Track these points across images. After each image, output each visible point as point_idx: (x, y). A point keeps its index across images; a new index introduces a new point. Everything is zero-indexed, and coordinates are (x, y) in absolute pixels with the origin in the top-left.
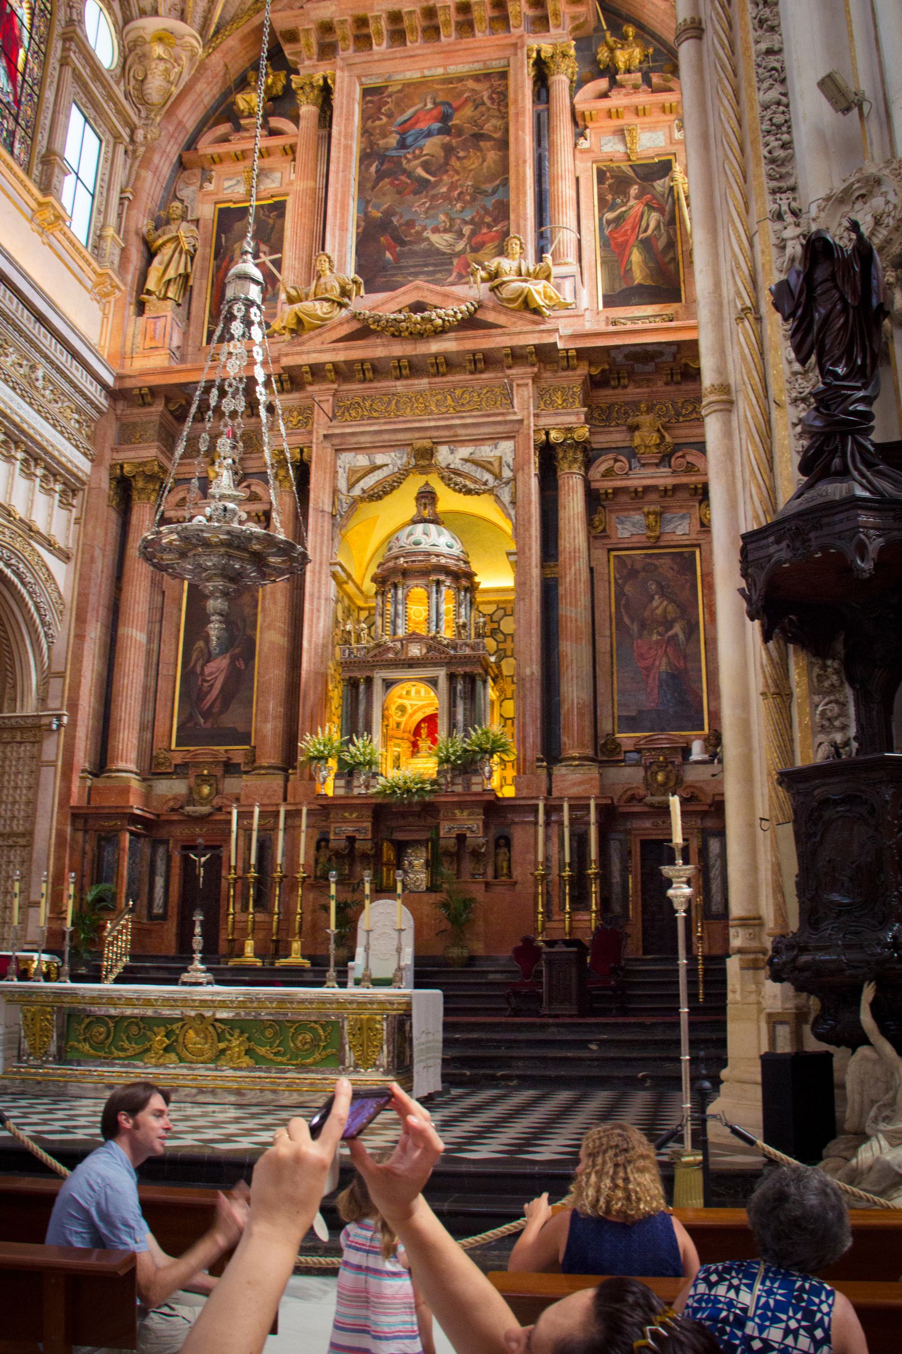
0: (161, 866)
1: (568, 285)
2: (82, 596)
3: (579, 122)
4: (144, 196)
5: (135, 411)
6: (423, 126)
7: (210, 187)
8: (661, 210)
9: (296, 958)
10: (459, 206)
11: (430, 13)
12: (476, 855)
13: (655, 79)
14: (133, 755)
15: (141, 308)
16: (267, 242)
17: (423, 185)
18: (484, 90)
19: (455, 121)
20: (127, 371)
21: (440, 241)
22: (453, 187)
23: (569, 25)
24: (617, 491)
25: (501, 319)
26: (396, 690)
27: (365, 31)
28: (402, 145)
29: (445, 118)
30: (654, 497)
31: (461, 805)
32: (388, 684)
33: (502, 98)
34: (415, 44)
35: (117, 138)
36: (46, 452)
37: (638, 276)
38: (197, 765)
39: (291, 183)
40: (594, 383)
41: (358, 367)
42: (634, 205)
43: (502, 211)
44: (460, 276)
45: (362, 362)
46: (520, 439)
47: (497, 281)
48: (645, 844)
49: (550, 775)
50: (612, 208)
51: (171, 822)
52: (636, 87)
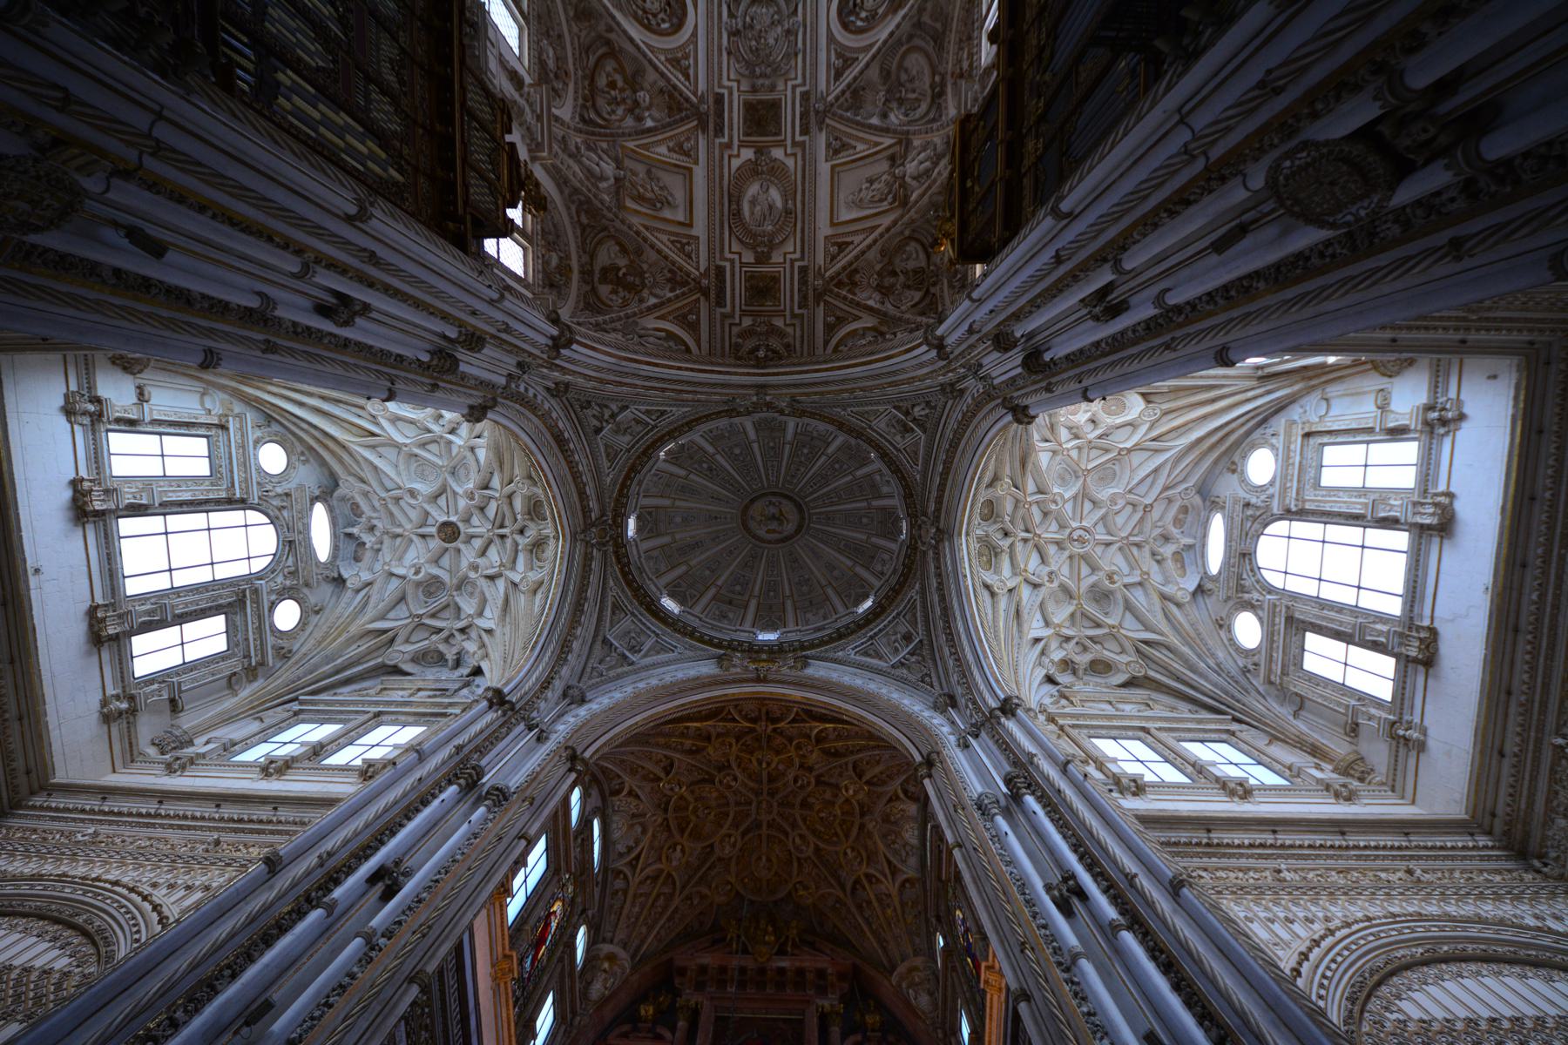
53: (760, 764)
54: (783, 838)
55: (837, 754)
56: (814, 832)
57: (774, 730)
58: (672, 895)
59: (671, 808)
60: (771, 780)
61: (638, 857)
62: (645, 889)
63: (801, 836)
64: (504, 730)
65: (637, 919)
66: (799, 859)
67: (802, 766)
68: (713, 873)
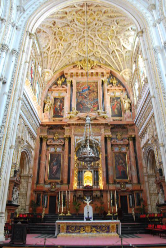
0: (46, 199)
1: (108, 114)
2: (36, 155)
3: (108, 90)
4: (44, 95)
5: (44, 128)
6: (86, 89)
7: (53, 94)
8: (119, 104)
9: (69, 214)
10: (91, 101)
11: (87, 73)
12: (99, 198)
13: (119, 85)
14: (43, 182)
15: (44, 112)
16: (62, 103)
17: (86, 98)
18: (94, 84)
19: (90, 89)
20: (42, 121)
21: (89, 106)
22: (90, 98)
23: (106, 77)
24: (115, 144)
25: (100, 119)
26: (86, 173)
27: (77, 74)
28: (83, 91)
29: (89, 88)
30: (120, 145)
31: (97, 190)
32: (85, 172)
33: (97, 86)
34: (85, 77)
35: (41, 86)
36: (33, 134)
37: (116, 113)
38: (52, 183)
39: (66, 95)
40: (111, 129)
41: (79, 124)
42: (115, 103)
43: (97, 102)
44: (92, 111)
45: (79, 124)
46: (102, 136)
47: (99, 114)
48: (121, 196)
49: (108, 186)
50: (112, 103)
51: (48, 192)
52: (116, 86)
53: (84, 20)
54: (92, 40)
55: (110, 17)
56: (101, 38)
57: (89, 9)
58: (60, 56)
59: (56, 34)
60: (88, 24)
61: (49, 48)
62: (53, 55)
63: (97, 40)
64: (7, 30)
65: (52, 63)
66: (96, 46)
67: (98, 20)
68: (71, 50)
